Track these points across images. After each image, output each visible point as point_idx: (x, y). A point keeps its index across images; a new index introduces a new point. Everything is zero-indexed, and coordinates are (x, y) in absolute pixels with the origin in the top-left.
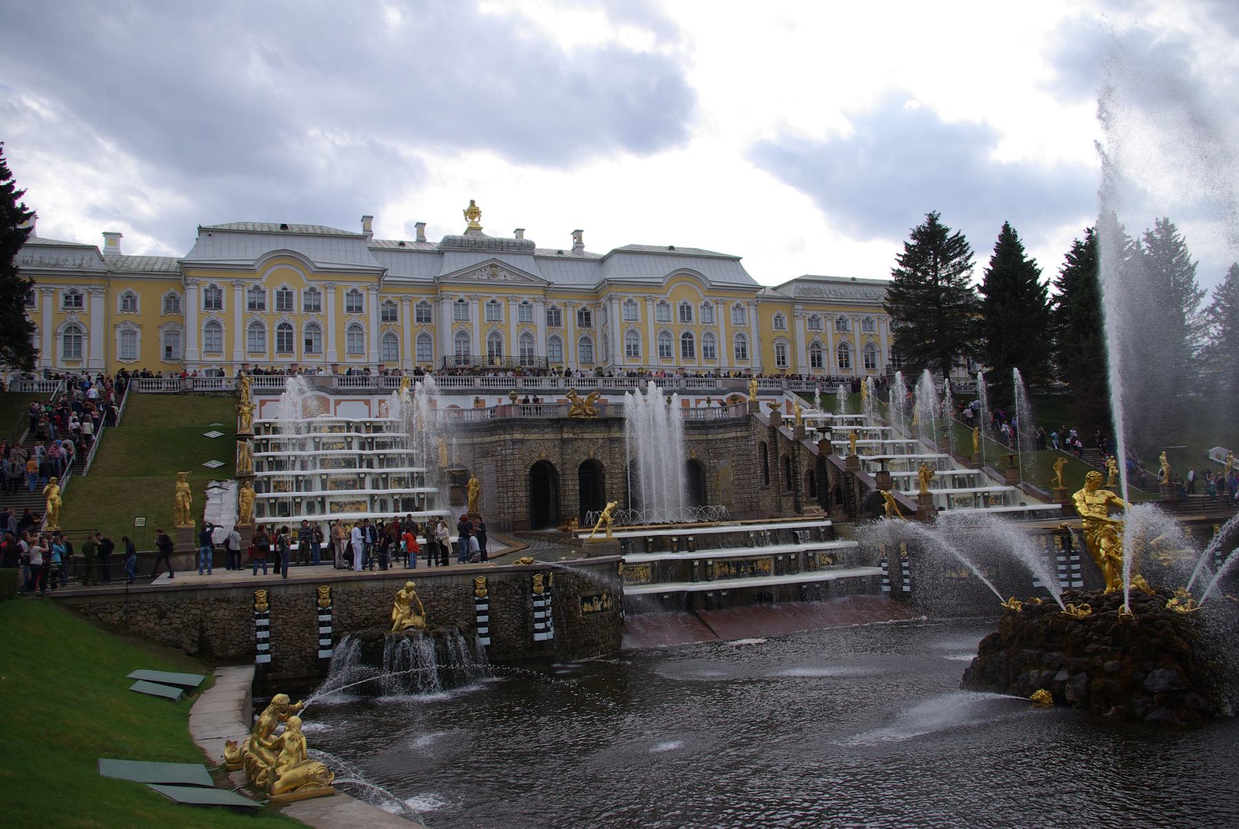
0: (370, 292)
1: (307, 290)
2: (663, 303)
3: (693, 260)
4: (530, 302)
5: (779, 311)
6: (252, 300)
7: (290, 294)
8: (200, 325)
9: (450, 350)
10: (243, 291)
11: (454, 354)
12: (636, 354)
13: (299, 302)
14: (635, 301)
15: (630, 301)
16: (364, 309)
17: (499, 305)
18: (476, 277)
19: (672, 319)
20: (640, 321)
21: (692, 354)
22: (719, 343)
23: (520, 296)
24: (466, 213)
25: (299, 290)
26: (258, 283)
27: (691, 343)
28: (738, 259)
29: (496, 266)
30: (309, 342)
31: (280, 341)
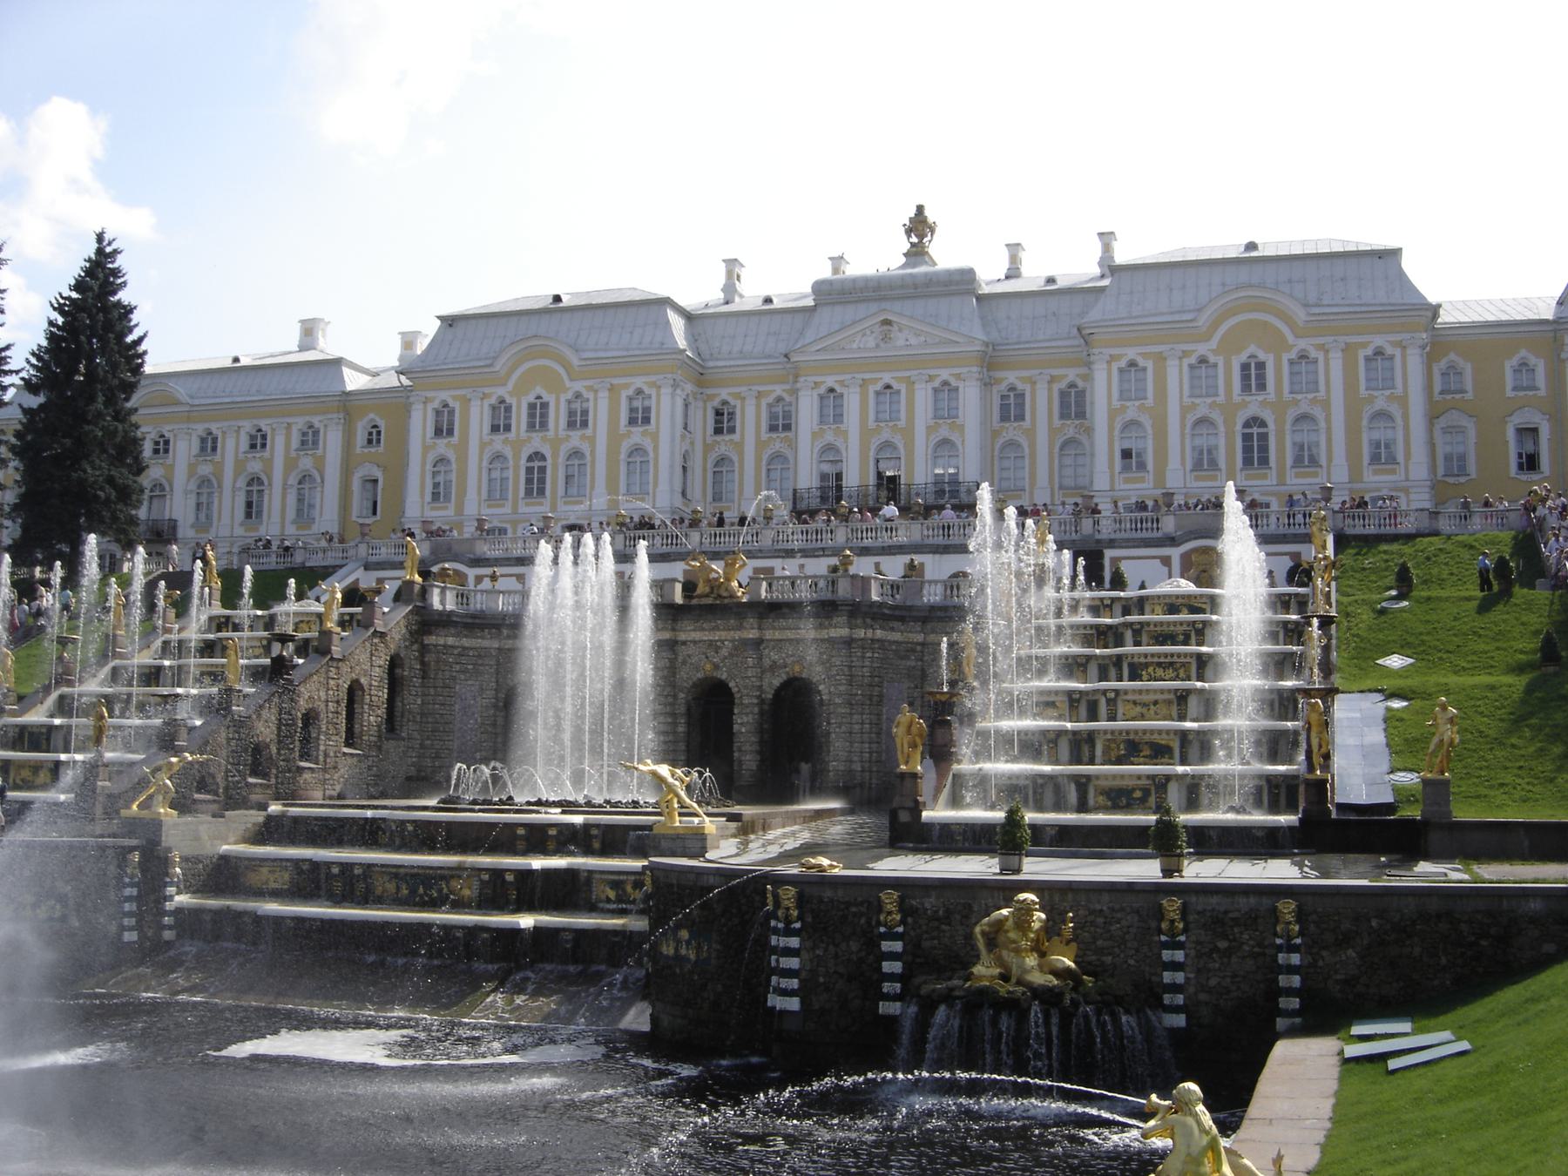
1: (569, 395)
2: (1203, 360)
4: (954, 383)
6: (496, 423)
7: (545, 406)
8: (424, 464)
9: (807, 478)
10: (482, 406)
12: (1142, 466)
13: (557, 417)
14: (1141, 362)
15: (1132, 364)
16: (653, 421)
17: (898, 392)
18: (855, 346)
19: (1221, 391)
21: (1264, 461)
22: (1329, 429)
23: (933, 372)
24: (909, 232)
26: (501, 392)
27: (1264, 437)
28: (1395, 254)
30: (568, 478)
31: (529, 481)
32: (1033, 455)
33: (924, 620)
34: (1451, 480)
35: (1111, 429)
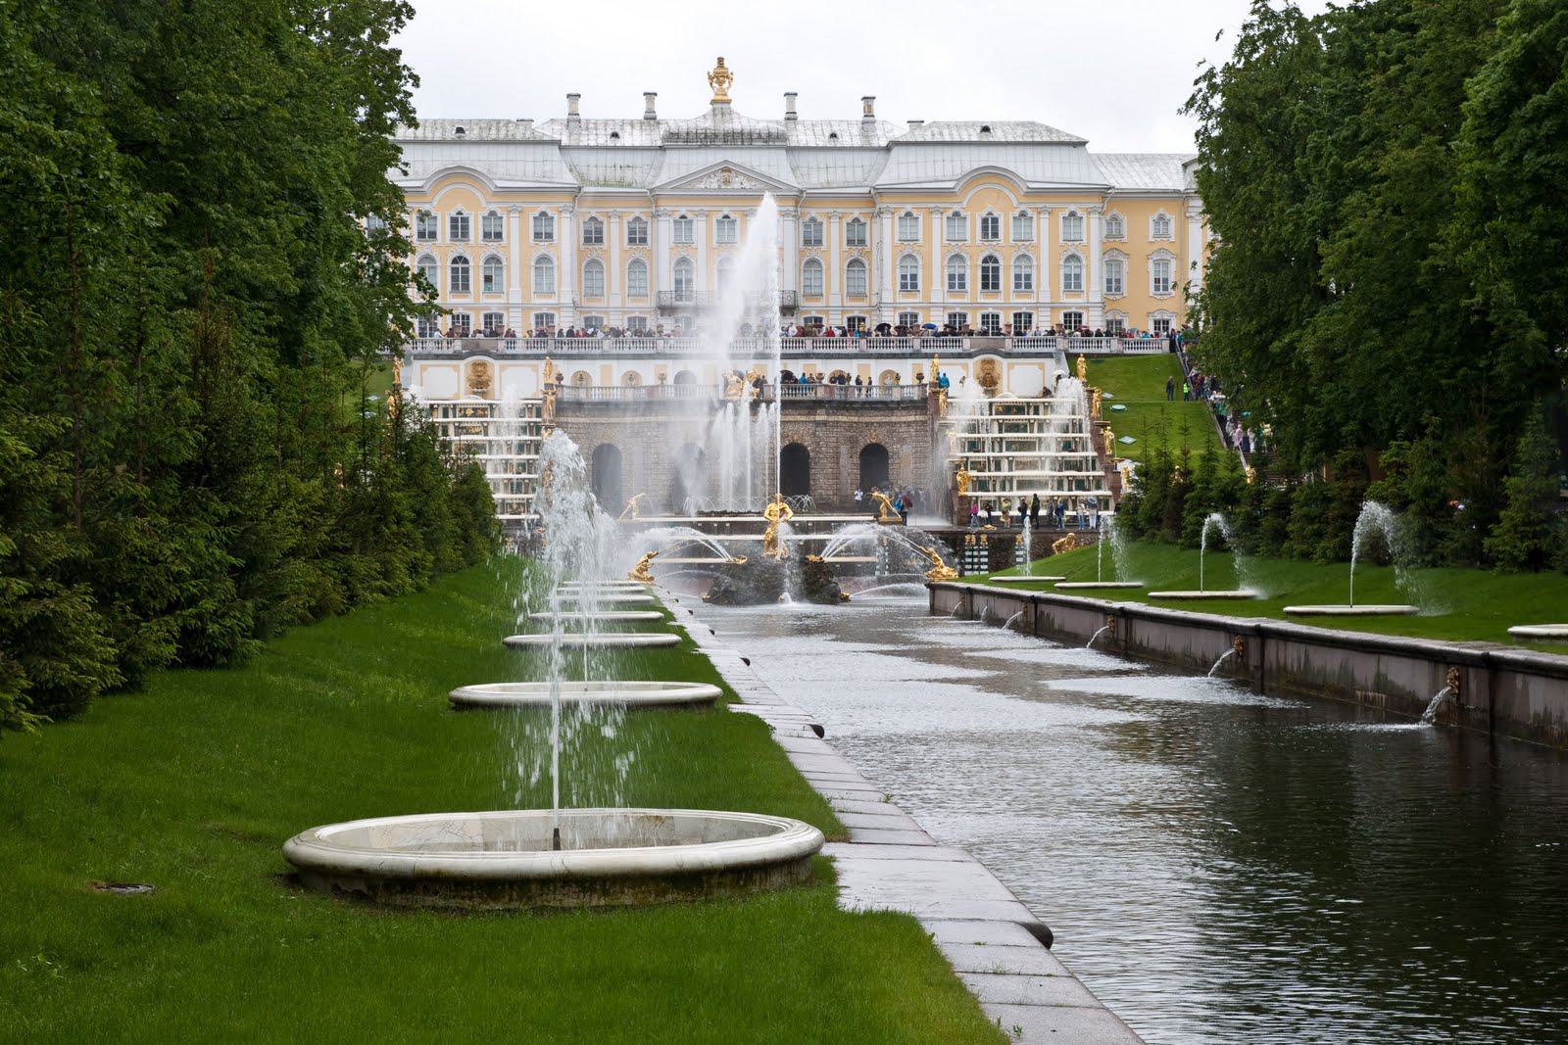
0: (563, 215)
3: (1002, 150)
5: (1161, 211)
7: (465, 220)
11: (673, 289)
12: (914, 286)
13: (476, 230)
17: (734, 222)
19: (968, 237)
20: (921, 242)
21: (996, 286)
22: (1038, 267)
24: (711, 78)
25: (476, 216)
27: (996, 270)
28: (1083, 144)
29: (729, 170)
30: (488, 279)
31: (454, 279)
32: (829, 268)
33: (857, 410)
34: (1111, 297)
35: (894, 260)
